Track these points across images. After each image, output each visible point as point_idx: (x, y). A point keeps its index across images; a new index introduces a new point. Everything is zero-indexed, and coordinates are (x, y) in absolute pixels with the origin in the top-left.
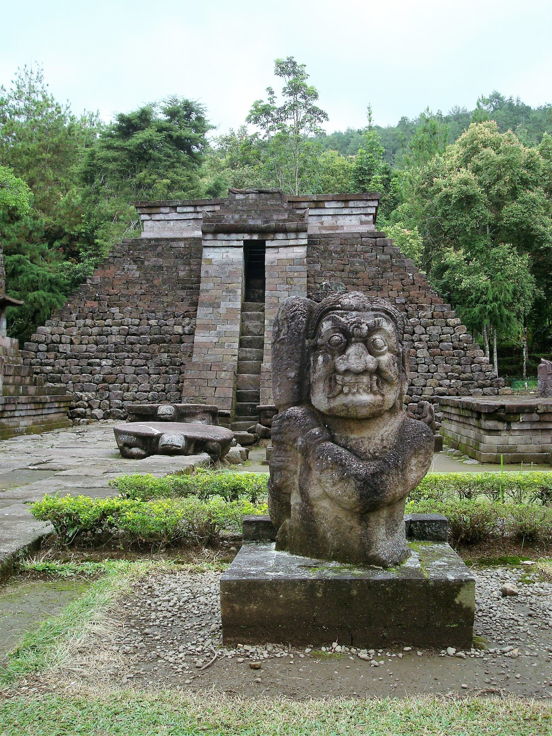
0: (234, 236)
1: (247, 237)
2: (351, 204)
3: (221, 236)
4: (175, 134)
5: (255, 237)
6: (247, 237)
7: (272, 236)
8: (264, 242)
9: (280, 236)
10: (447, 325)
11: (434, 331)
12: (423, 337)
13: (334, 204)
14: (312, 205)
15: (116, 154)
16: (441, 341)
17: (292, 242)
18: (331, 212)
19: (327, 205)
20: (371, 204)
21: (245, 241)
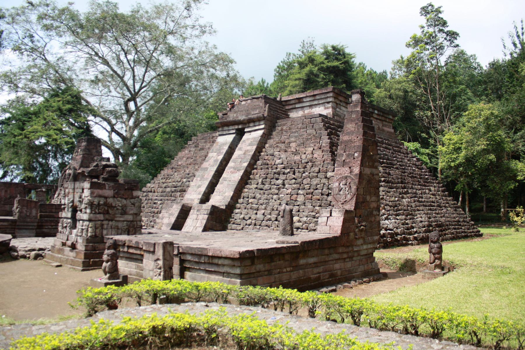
0: (231, 128)
1: (236, 127)
2: (318, 97)
3: (226, 128)
4: (324, 66)
5: (240, 127)
6: (236, 127)
7: (247, 125)
8: (244, 129)
9: (252, 125)
10: (326, 177)
11: (315, 181)
12: (306, 186)
13: (308, 99)
14: (297, 101)
15: (297, 82)
16: (317, 189)
17: (257, 128)
18: (308, 104)
19: (305, 100)
20: (328, 95)
21: (237, 130)
